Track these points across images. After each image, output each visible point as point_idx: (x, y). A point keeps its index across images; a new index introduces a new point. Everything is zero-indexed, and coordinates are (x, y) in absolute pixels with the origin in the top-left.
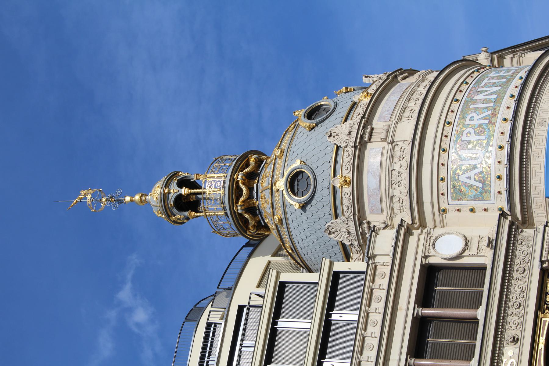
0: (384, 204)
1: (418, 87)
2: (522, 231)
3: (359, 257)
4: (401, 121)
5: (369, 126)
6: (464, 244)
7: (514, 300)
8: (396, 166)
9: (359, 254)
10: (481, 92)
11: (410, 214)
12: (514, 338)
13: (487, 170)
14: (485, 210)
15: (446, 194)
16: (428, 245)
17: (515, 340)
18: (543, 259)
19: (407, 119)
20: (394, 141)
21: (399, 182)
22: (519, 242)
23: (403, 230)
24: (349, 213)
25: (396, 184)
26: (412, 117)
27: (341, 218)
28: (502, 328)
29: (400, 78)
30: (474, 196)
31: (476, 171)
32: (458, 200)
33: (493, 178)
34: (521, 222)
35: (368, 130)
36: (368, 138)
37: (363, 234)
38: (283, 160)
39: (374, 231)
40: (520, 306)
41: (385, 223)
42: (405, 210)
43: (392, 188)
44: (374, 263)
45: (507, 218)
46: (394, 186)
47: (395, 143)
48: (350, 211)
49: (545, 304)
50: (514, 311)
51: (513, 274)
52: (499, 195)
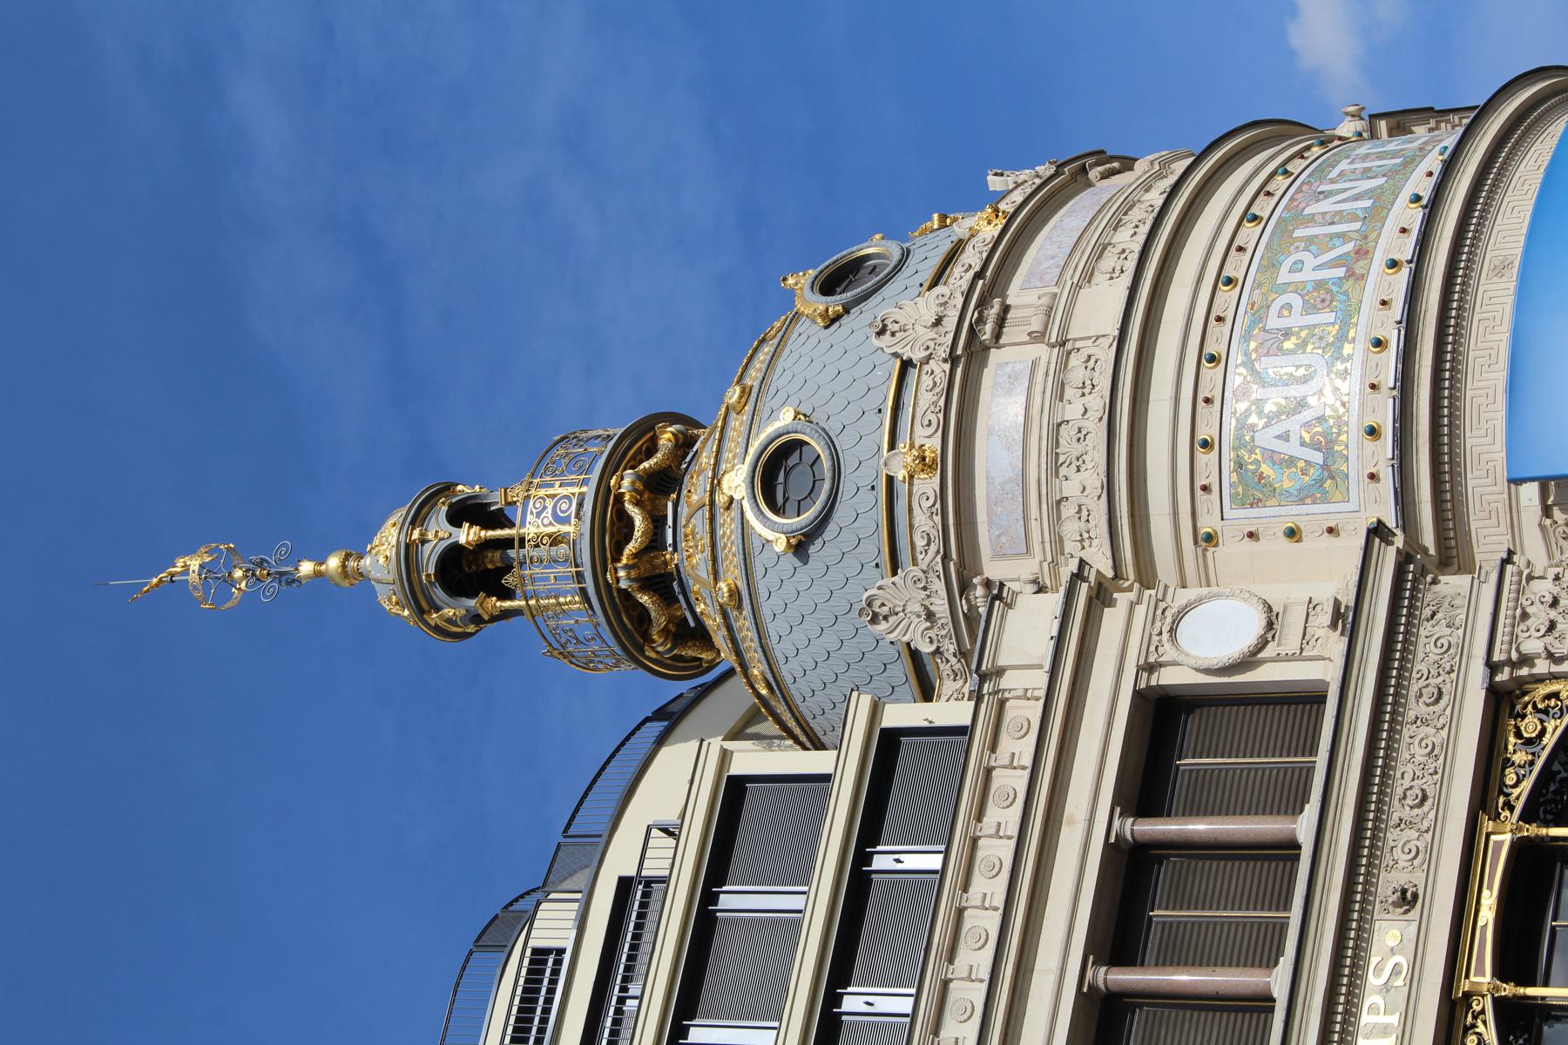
0: (1034, 525)
1: (1147, 191)
2: (1435, 582)
3: (959, 691)
4: (1089, 282)
5: (997, 302)
6: (1264, 623)
7: (1407, 783)
8: (1072, 411)
9: (960, 682)
10: (1326, 195)
11: (1109, 553)
12: (1404, 892)
13: (1336, 411)
14: (1330, 530)
15: (1215, 488)
16: (1156, 631)
17: (1407, 900)
18: (1496, 657)
19: (1108, 276)
20: (1069, 340)
21: (1078, 459)
22: (1427, 612)
23: (1083, 591)
24: (930, 557)
25: (1071, 463)
26: (1122, 272)
27: (909, 571)
28: (1369, 864)
29: (1094, 174)
30: (1300, 490)
31: (1307, 415)
32: (1252, 505)
33: (1352, 436)
34: (1436, 560)
35: (993, 311)
36: (992, 334)
37: (971, 618)
38: (745, 417)
39: (999, 597)
40: (1424, 798)
41: (1035, 581)
42: (1095, 542)
43: (1057, 477)
44: (996, 692)
45: (1390, 543)
46: (1063, 471)
47: (1069, 346)
48: (933, 548)
49: (1501, 792)
50: (1406, 813)
51: (1404, 706)
52: (1373, 485)
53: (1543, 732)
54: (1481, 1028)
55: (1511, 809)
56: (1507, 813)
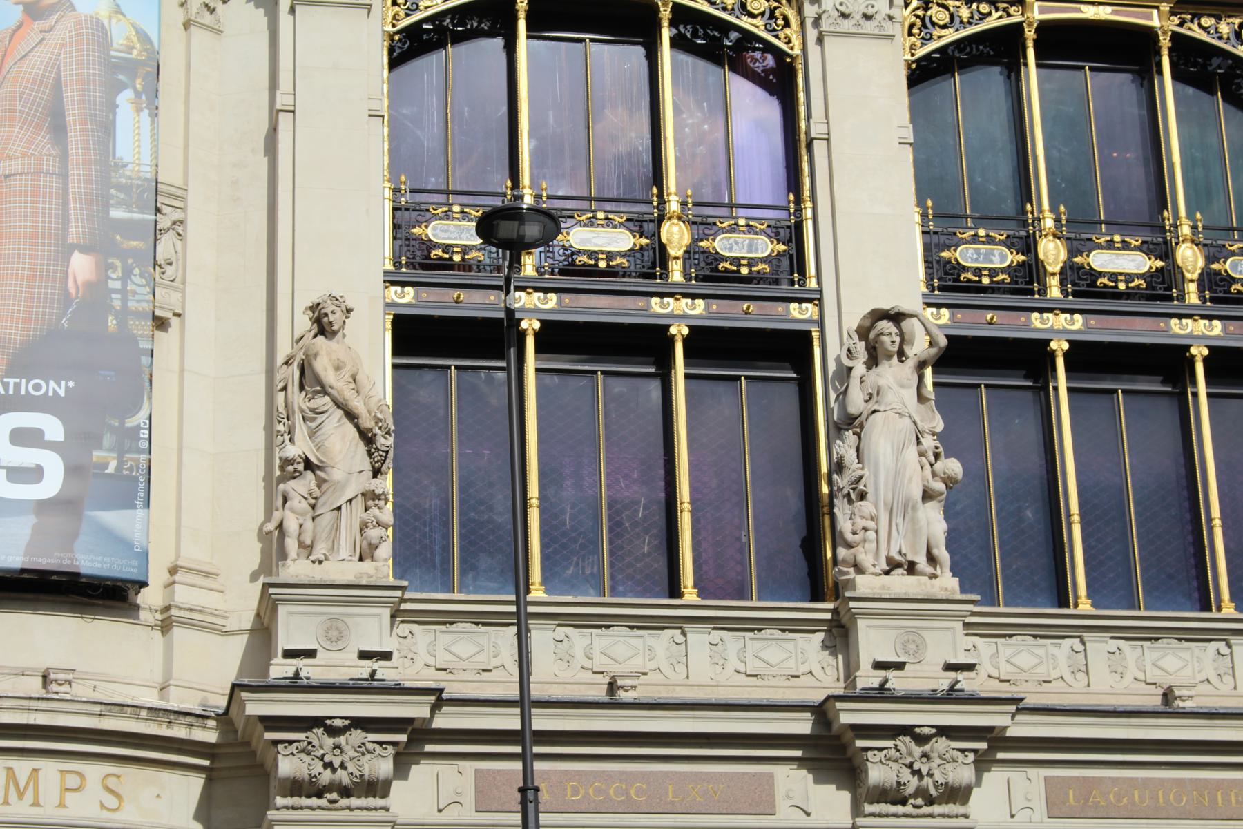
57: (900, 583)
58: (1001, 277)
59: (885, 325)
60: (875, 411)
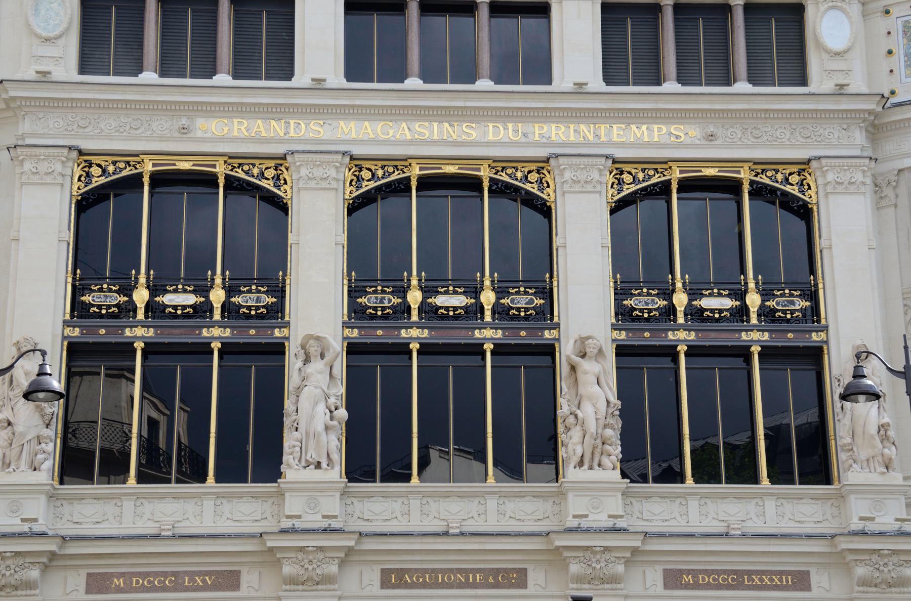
32: (904, 31)
53: (792, 185)
54: (657, 176)
55: (756, 176)
56: (754, 174)
57: (312, 474)
58: (388, 311)
59: (311, 342)
60: (306, 386)
